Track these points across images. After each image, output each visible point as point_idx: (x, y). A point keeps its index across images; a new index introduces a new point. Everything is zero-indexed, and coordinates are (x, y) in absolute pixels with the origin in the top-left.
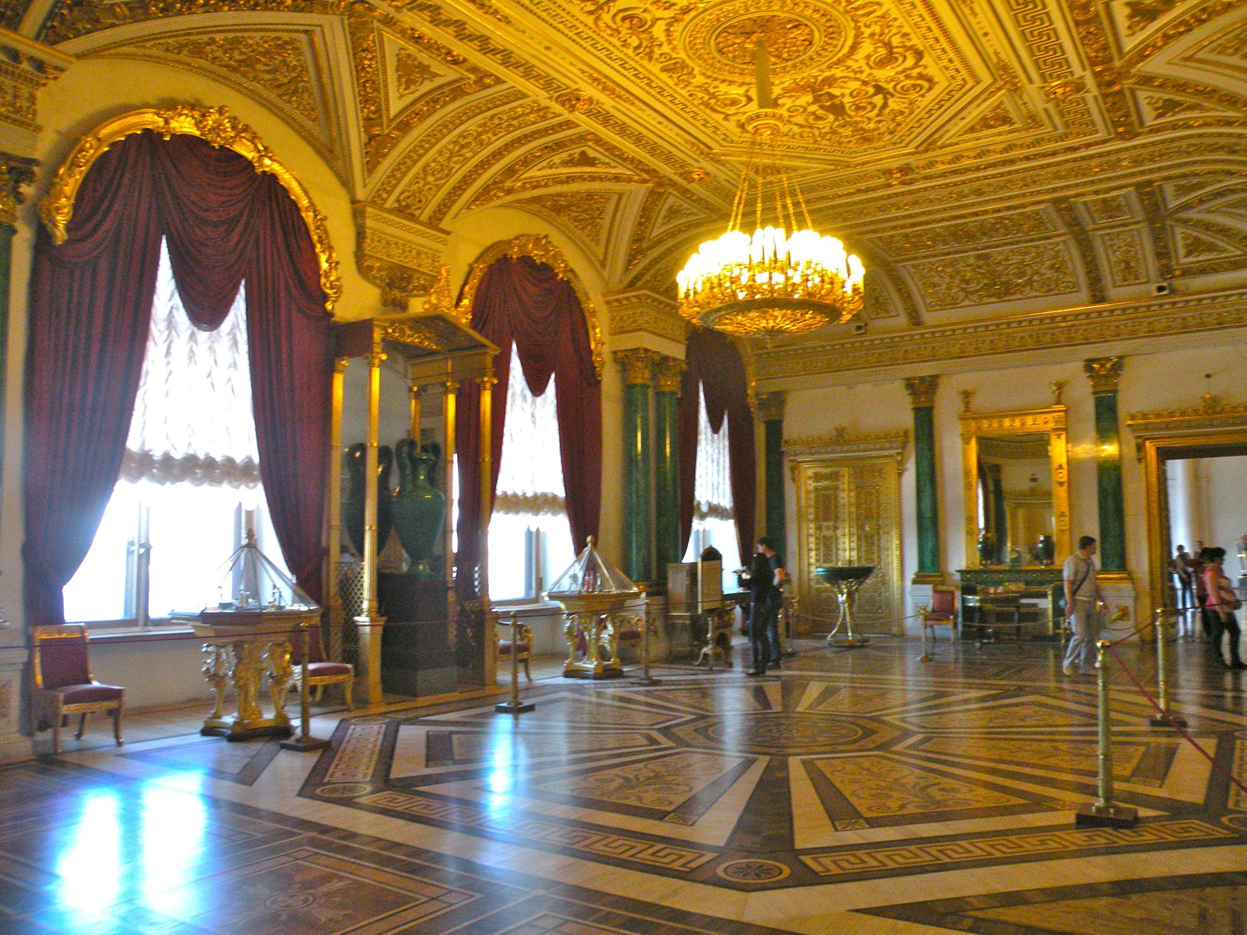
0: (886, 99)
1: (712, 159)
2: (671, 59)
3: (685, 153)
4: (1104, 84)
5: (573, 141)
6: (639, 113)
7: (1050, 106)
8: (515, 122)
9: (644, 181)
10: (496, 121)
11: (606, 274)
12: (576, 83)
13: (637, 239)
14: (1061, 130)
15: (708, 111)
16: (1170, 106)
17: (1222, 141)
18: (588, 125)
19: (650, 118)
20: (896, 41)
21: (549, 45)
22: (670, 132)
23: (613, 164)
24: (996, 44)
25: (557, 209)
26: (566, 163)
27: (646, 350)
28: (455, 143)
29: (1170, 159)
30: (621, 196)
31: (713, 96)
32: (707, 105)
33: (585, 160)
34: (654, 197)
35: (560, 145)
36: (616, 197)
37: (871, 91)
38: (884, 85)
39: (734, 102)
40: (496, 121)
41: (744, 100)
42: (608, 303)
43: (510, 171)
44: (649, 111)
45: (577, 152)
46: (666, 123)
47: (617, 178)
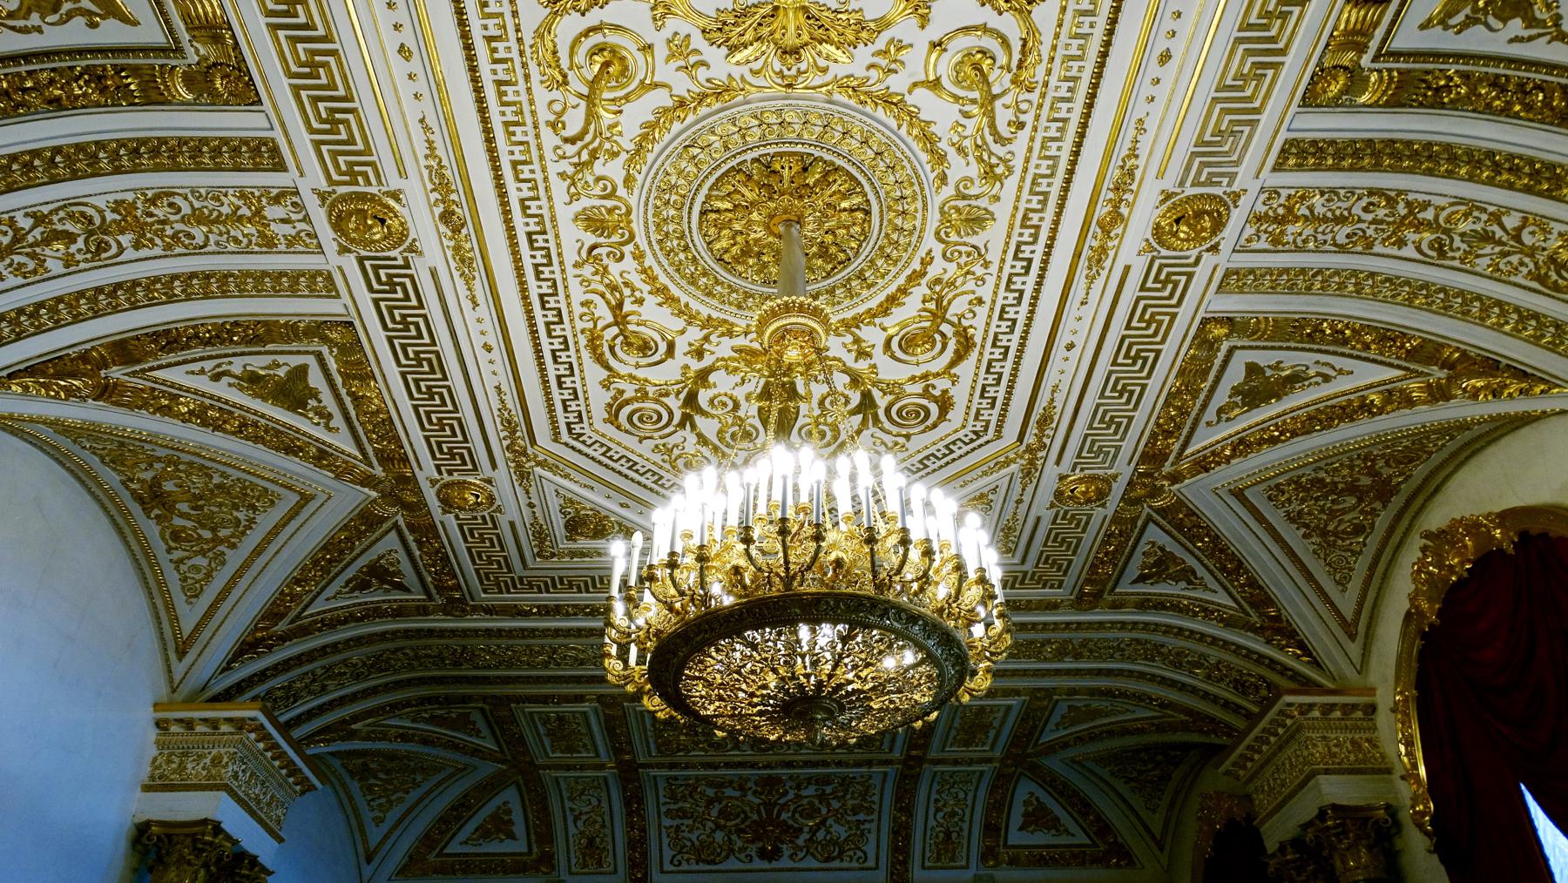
0: (864, 422)
1: (519, 466)
2: (612, 195)
3: (485, 434)
4: (1129, 500)
5: (289, 332)
6: (467, 305)
7: (1048, 516)
8: (199, 232)
9: (367, 481)
10: (160, 212)
11: (179, 668)
12: (402, 174)
13: (273, 613)
14: (1029, 567)
15: (586, 355)
16: (1161, 567)
17: (1172, 642)
18: (357, 299)
19: (476, 326)
20: (958, 307)
21: (411, 44)
22: (490, 374)
23: (338, 421)
24: (1065, 371)
25: (154, 498)
26: (252, 381)
27: (217, 828)
28: (39, 219)
29: (1100, 658)
30: (306, 499)
31: (620, 319)
32: (593, 344)
33: (292, 392)
34: (367, 521)
35: (260, 333)
36: (295, 498)
37: (856, 398)
38: (876, 393)
39: (645, 348)
40: (160, 212)
41: (663, 347)
42: (161, 725)
43: (124, 350)
44: (485, 310)
45: (280, 362)
46: (498, 354)
47: (322, 456)
